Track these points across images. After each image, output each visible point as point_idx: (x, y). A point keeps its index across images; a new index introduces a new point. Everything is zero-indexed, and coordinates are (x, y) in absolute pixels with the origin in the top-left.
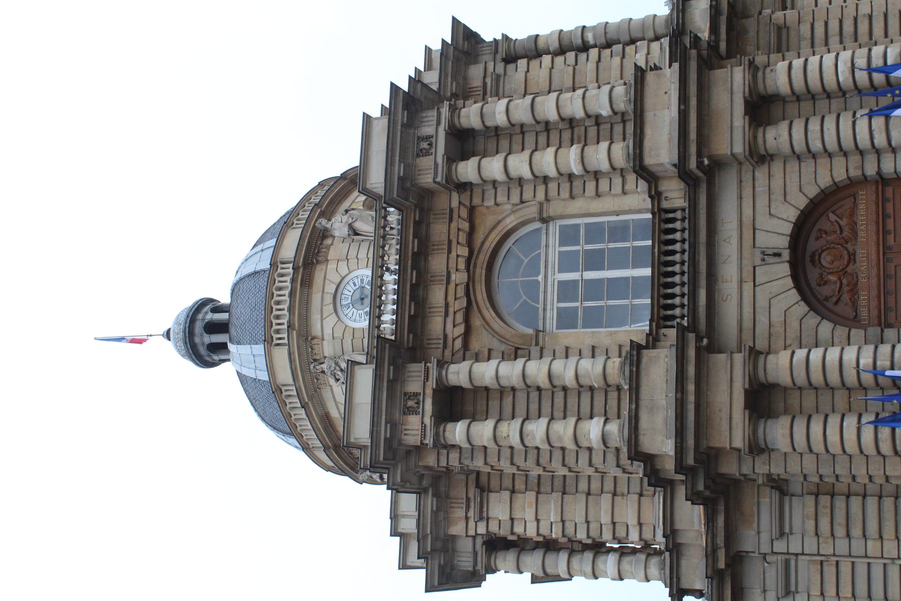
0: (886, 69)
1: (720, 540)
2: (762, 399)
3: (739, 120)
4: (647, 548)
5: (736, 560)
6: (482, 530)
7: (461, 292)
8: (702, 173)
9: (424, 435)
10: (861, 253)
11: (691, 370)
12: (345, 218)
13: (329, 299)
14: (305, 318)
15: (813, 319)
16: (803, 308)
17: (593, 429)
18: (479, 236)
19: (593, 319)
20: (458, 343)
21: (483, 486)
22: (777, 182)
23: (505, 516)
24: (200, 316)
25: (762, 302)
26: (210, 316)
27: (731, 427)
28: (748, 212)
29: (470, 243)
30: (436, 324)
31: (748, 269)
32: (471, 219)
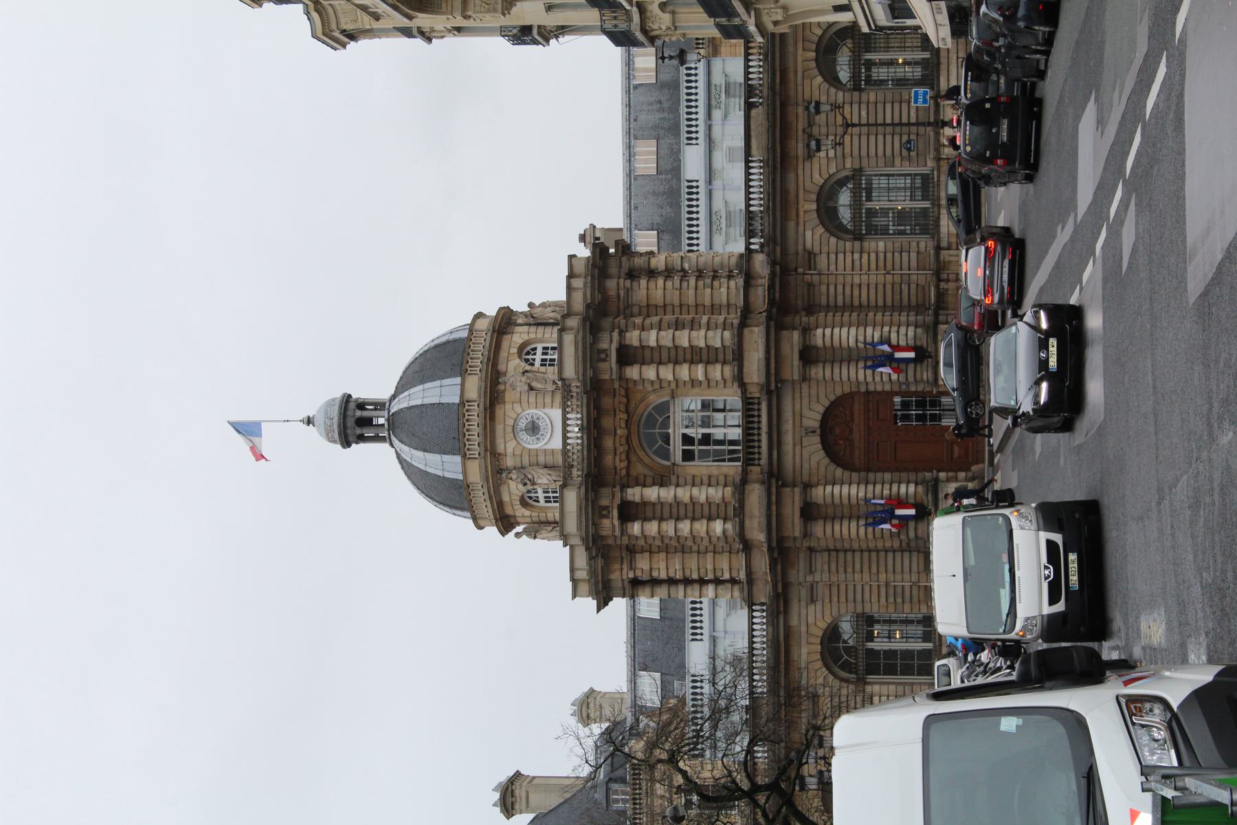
0: (873, 345)
1: (779, 578)
2: (809, 512)
3: (796, 362)
4: (733, 581)
5: (786, 585)
6: (631, 575)
7: (623, 441)
8: (774, 387)
9: (614, 531)
10: (855, 429)
11: (774, 498)
12: (524, 379)
13: (509, 430)
14: (493, 442)
15: (832, 467)
16: (827, 460)
17: (718, 527)
18: (633, 405)
19: (704, 455)
20: (624, 472)
21: (632, 551)
22: (814, 392)
23: (646, 567)
24: (349, 413)
25: (806, 456)
26: (359, 413)
27: (794, 526)
28: (798, 407)
29: (627, 411)
30: (608, 460)
31: (798, 438)
32: (627, 396)
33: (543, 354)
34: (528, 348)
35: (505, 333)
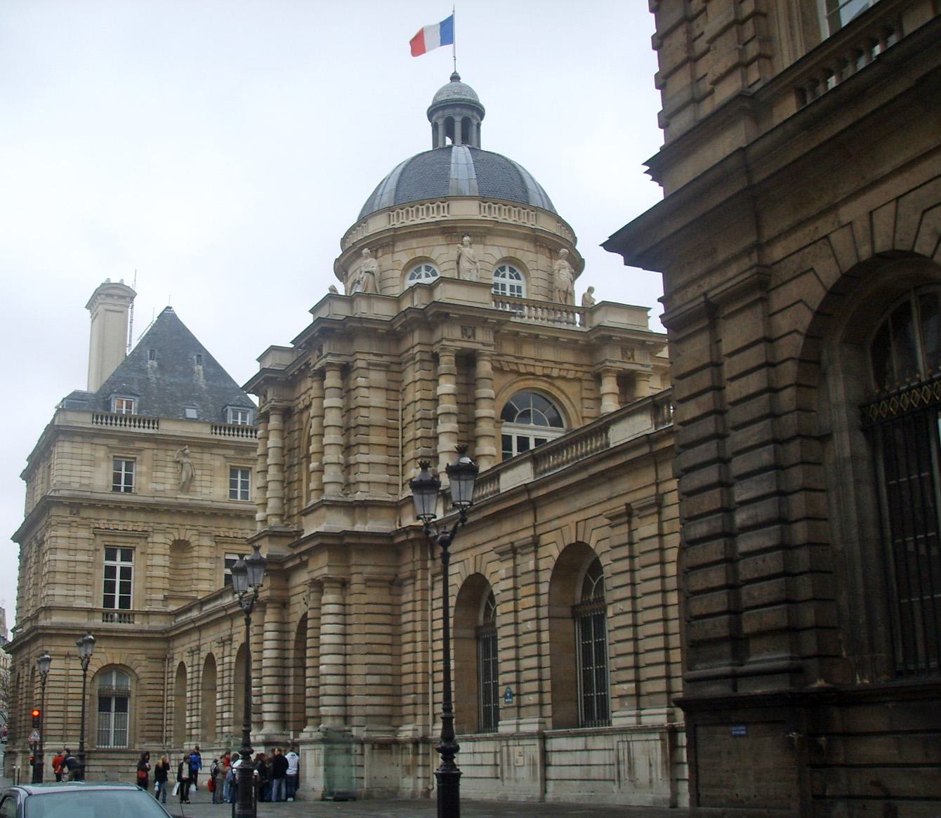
24: (458, 110)
26: (458, 119)
33: (512, 287)
34: (518, 271)
35: (536, 245)
